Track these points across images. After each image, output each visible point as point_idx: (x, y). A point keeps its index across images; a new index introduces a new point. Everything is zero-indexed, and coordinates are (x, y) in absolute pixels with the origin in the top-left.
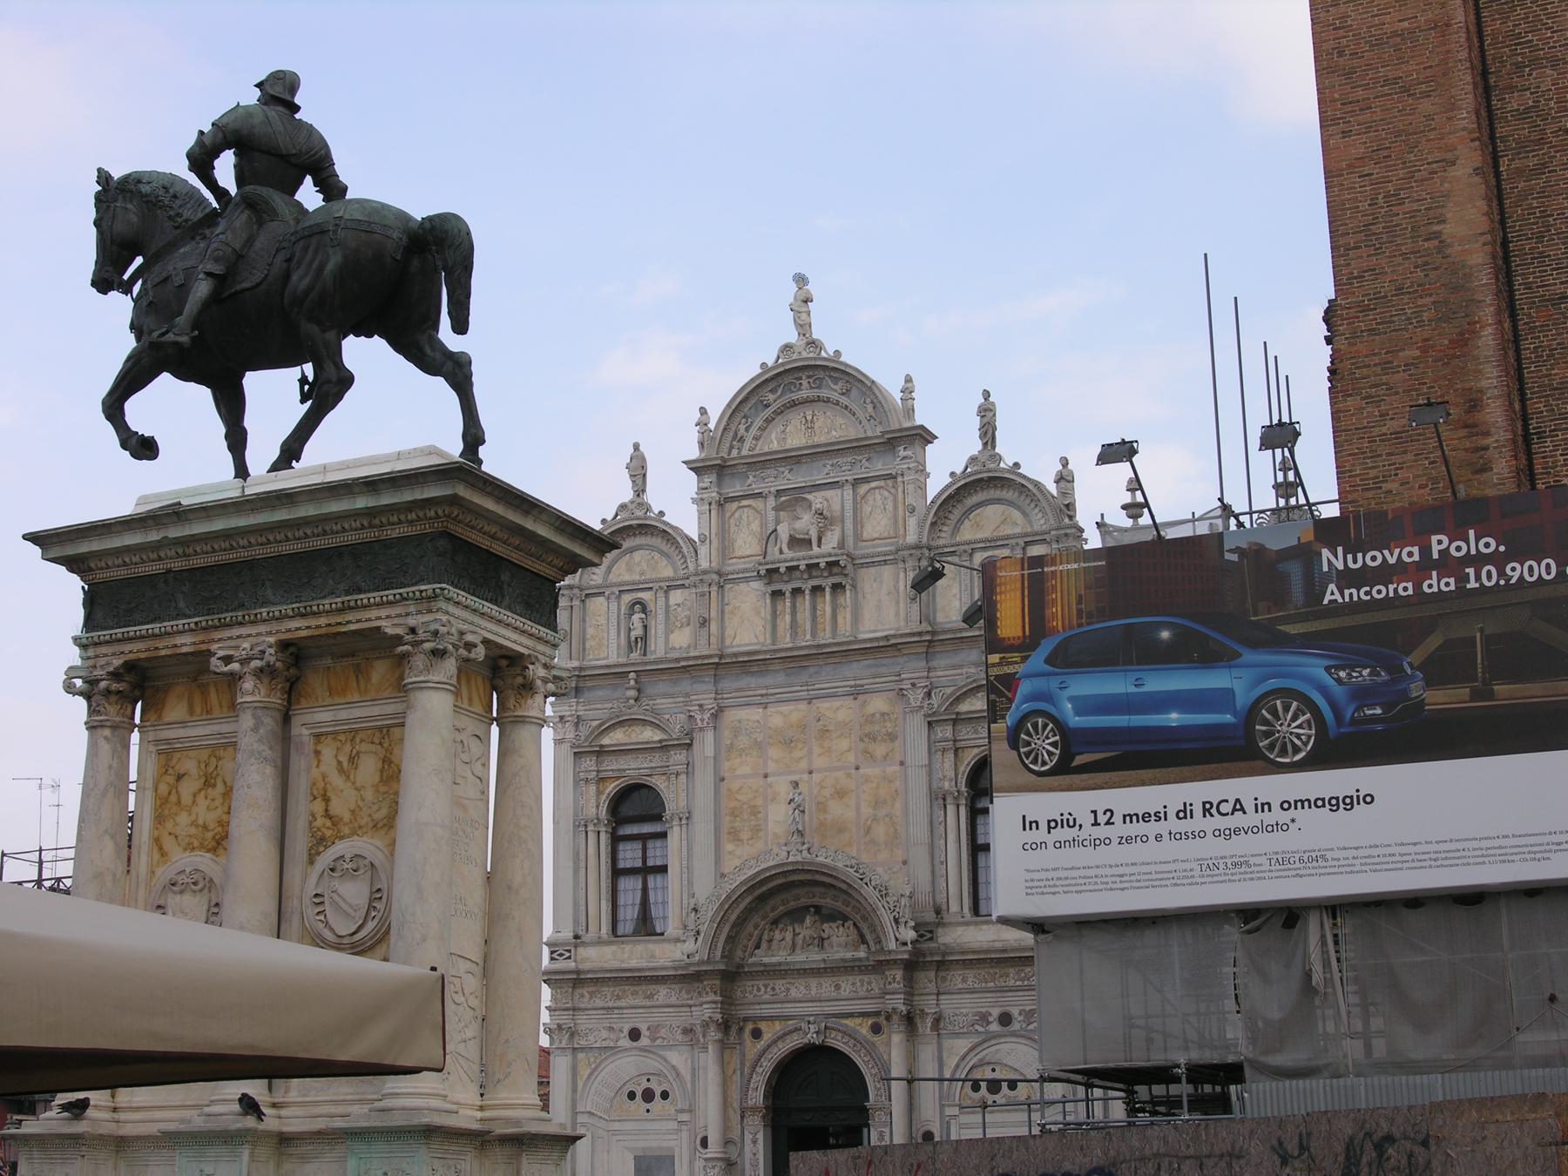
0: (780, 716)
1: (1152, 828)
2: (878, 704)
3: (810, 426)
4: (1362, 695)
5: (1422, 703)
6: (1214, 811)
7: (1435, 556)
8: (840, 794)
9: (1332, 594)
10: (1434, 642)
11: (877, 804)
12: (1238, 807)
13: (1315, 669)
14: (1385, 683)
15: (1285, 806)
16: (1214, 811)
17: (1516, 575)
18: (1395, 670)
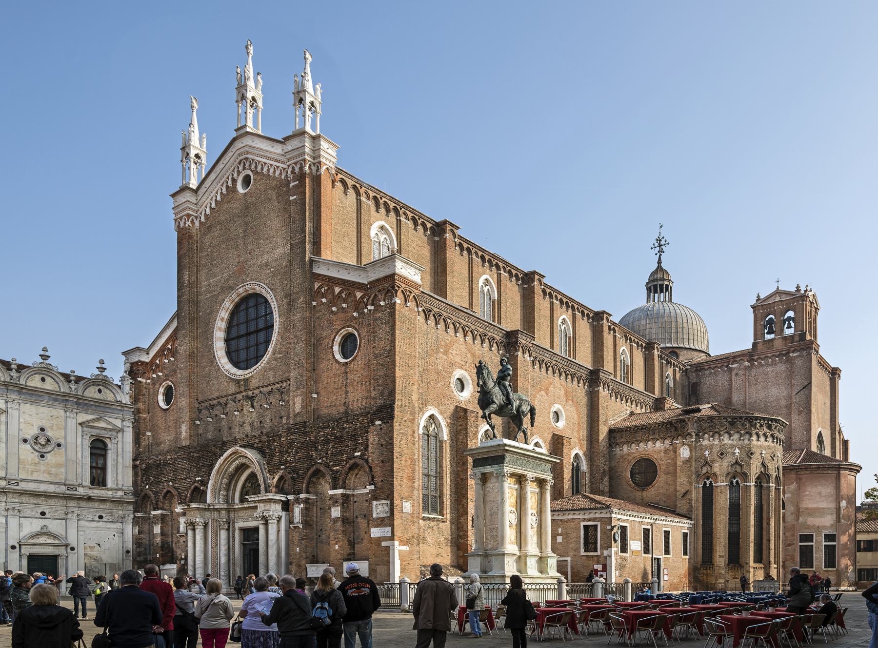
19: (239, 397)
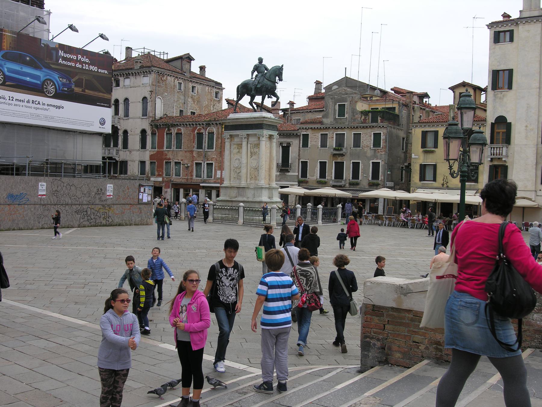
1: (21, 103)
4: (64, 85)
5: (74, 90)
6: (34, 103)
7: (79, 59)
9: (60, 61)
10: (77, 78)
12: (39, 103)
13: (56, 76)
14: (68, 83)
15: (48, 105)
16: (34, 103)
17: (91, 68)
18: (70, 81)
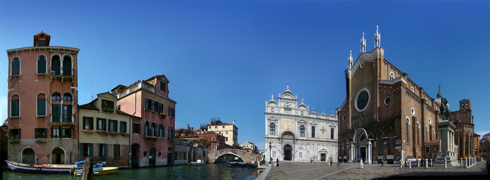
0: (285, 119)
2: (293, 120)
3: (288, 97)
8: (290, 126)
11: (293, 127)
19: (360, 116)
